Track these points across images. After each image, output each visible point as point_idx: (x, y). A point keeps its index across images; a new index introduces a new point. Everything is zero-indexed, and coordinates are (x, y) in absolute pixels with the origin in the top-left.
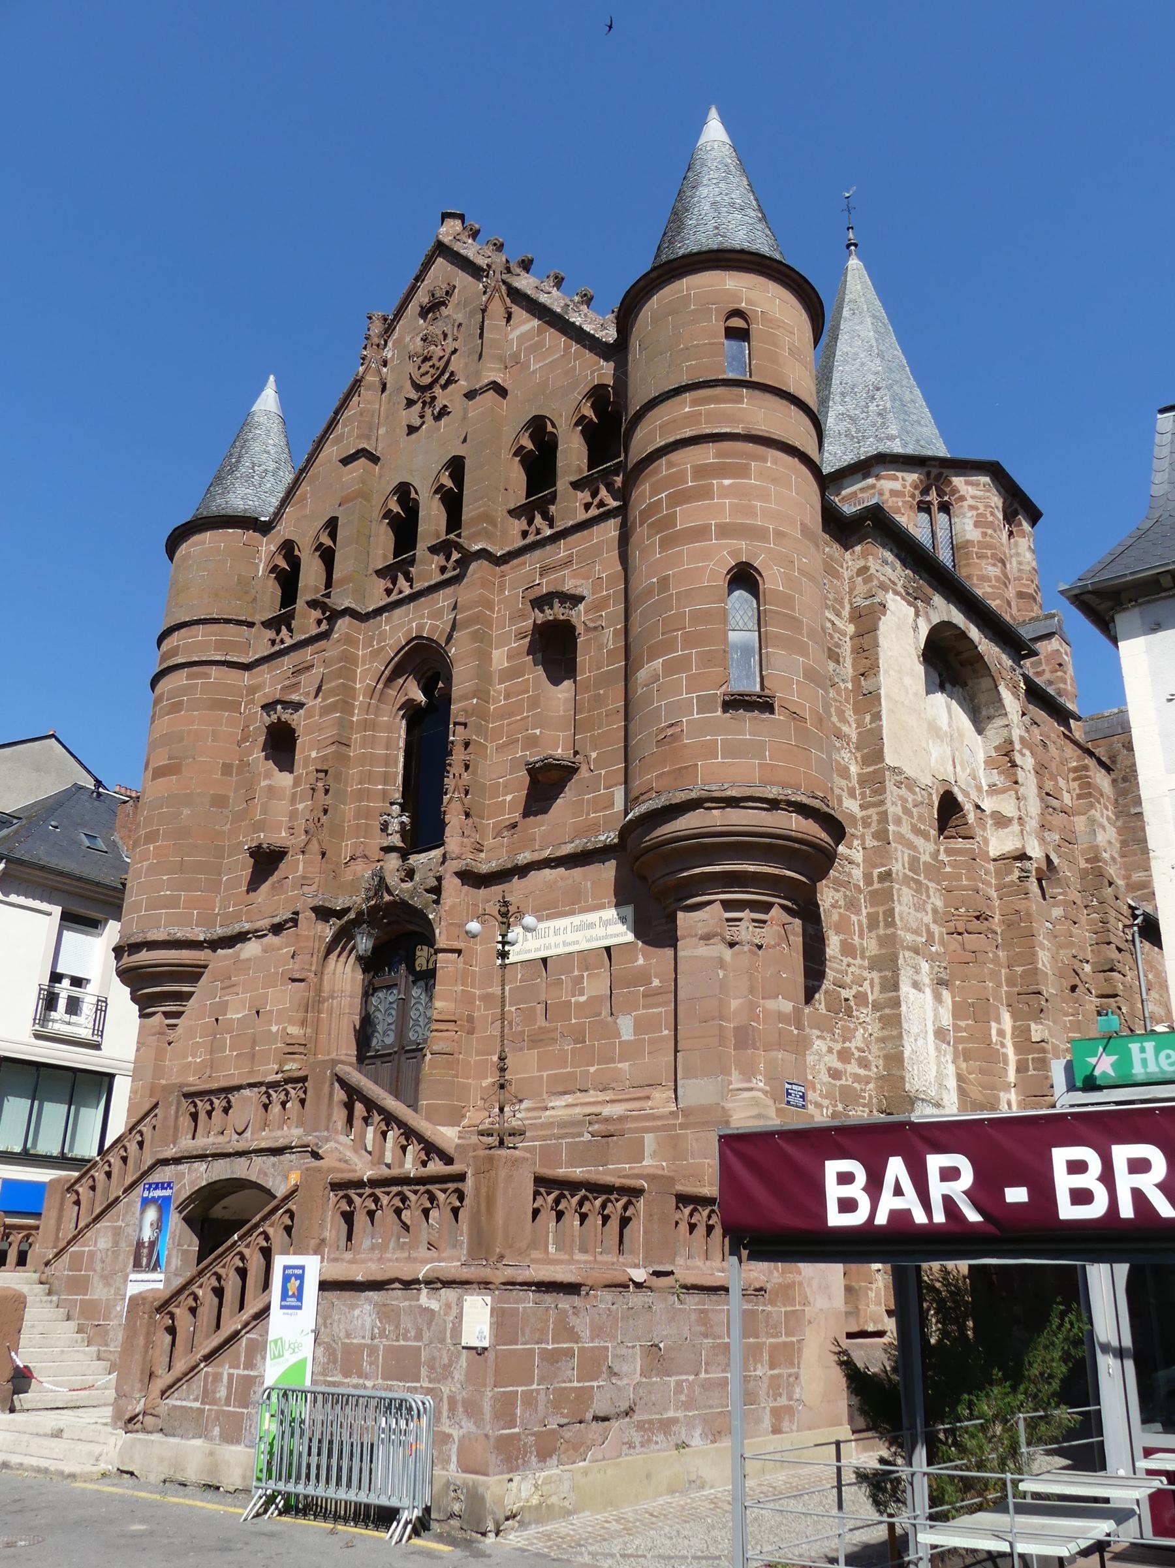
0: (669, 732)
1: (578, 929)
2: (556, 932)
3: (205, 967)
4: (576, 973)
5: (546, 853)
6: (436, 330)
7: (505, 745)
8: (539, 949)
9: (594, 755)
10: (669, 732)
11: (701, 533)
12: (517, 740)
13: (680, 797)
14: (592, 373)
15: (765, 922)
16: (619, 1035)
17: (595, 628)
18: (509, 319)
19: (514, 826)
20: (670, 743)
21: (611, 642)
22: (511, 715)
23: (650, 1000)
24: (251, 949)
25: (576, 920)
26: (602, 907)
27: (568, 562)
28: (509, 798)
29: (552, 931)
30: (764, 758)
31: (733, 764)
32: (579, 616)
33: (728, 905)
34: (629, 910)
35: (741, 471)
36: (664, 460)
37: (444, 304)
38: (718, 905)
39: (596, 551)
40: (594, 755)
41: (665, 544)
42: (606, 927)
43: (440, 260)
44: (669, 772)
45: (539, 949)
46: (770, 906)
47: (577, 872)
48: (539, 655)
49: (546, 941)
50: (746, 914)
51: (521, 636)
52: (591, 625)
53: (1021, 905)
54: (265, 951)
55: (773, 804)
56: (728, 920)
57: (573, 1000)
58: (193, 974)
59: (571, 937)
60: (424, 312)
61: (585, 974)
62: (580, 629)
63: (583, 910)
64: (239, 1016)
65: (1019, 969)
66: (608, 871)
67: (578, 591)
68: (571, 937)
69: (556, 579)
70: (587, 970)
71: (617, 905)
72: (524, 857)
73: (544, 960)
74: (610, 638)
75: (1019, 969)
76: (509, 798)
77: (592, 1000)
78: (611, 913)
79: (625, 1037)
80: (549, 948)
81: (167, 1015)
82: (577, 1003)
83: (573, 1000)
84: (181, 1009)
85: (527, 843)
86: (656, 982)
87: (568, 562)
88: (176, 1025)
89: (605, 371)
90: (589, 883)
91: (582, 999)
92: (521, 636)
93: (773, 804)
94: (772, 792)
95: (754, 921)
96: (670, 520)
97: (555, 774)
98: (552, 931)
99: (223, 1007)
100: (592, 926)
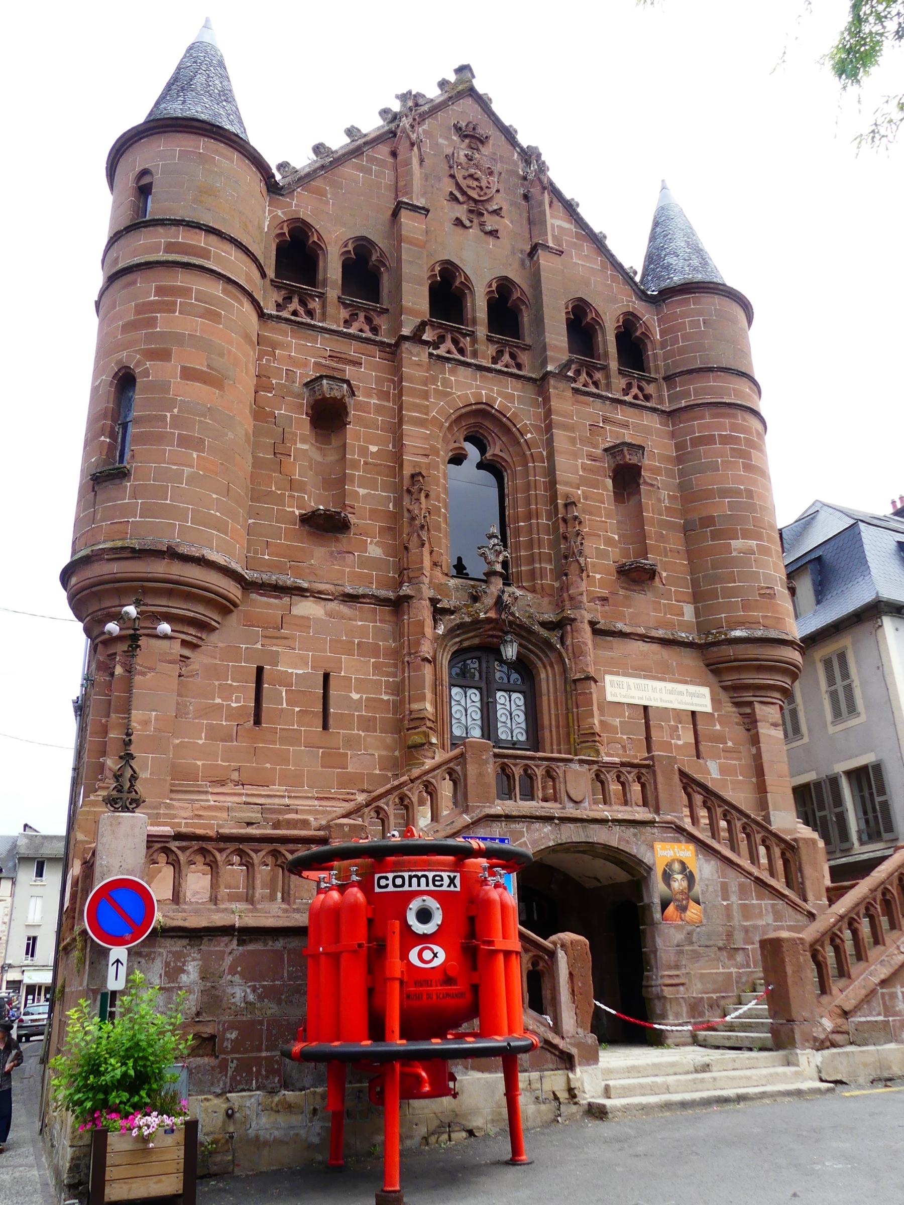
1: (671, 692)
2: (654, 690)
3: (235, 605)
5: (642, 631)
8: (642, 699)
12: (600, 536)
16: (709, 773)
21: (667, 501)
22: (591, 514)
23: (728, 755)
24: (306, 608)
25: (670, 686)
38: (778, 706)
40: (664, 574)
45: (642, 699)
54: (330, 614)
57: (673, 741)
58: (226, 607)
61: (680, 726)
64: (301, 672)
73: (646, 708)
77: (685, 744)
79: (714, 776)
81: (184, 643)
82: (676, 745)
83: (673, 741)
84: (200, 643)
86: (730, 744)
88: (188, 658)
91: (680, 743)
99: (274, 659)
100: (681, 693)
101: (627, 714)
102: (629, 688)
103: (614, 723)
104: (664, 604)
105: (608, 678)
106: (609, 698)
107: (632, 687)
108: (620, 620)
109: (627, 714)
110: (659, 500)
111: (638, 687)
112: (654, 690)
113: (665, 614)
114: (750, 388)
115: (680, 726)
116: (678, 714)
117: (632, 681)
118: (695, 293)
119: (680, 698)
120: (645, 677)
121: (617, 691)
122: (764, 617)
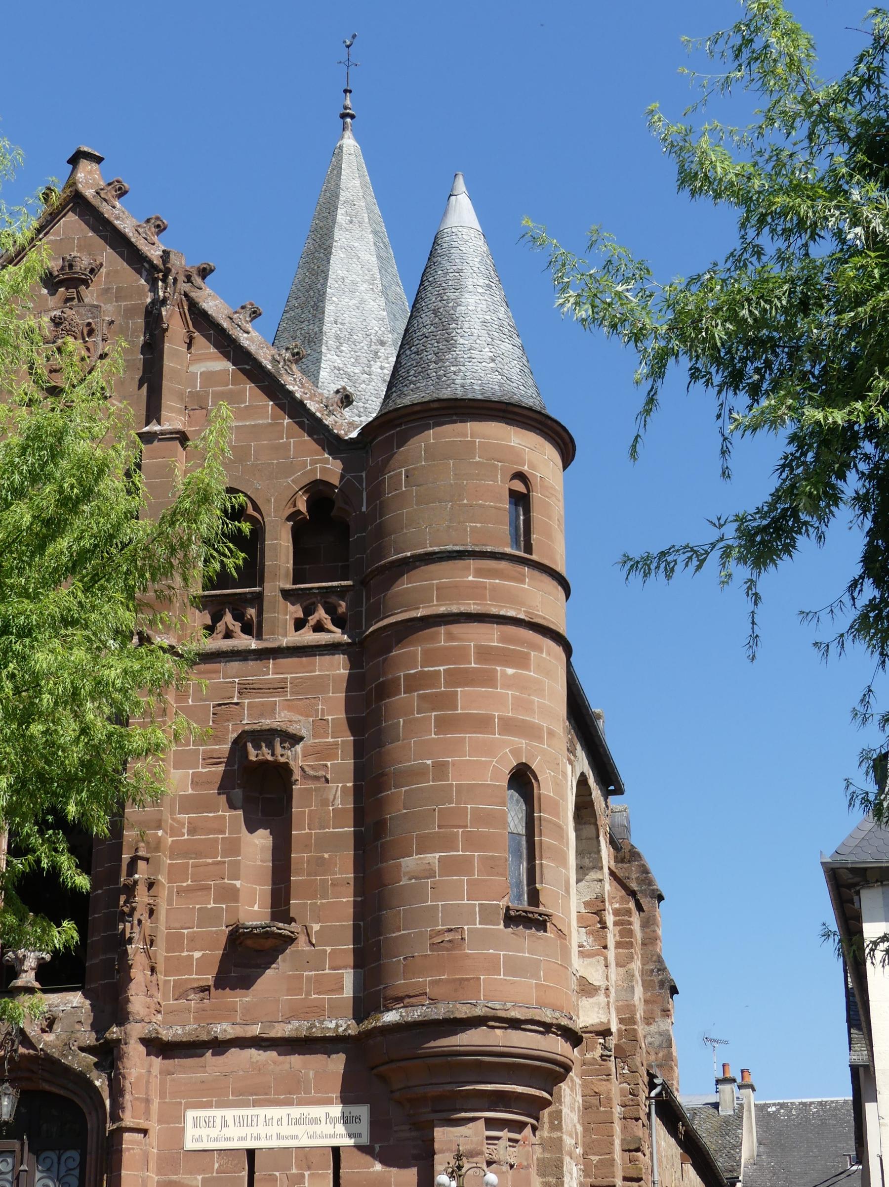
0: (448, 937)
1: (298, 1122)
2: (268, 1122)
4: (294, 1171)
5: (255, 1030)
6: (76, 317)
7: (188, 890)
8: (245, 1139)
9: (316, 927)
10: (448, 937)
11: (482, 723)
12: (208, 888)
13: (463, 1012)
14: (314, 462)
15: (517, 1141)
17: (316, 778)
18: (189, 346)
19: (205, 989)
20: (448, 950)
21: (338, 801)
25: (296, 1112)
26: (328, 1102)
27: (279, 688)
28: (197, 955)
29: (261, 1120)
30: (539, 978)
31: (514, 982)
32: (296, 757)
33: (491, 1124)
34: (363, 1111)
35: (521, 661)
36: (442, 629)
37: (86, 282)
39: (318, 686)
40: (316, 927)
41: (443, 724)
42: (320, 1123)
43: (71, 218)
44: (447, 981)
45: (245, 1139)
46: (523, 1125)
47: (296, 1060)
48: (238, 793)
49: (254, 1130)
50: (505, 1134)
51: (211, 760)
52: (312, 773)
53: (601, 1087)
55: (547, 1028)
56: (488, 1138)
59: (287, 1130)
60: (51, 282)
61: (307, 1174)
62: (297, 775)
63: (302, 1103)
65: (595, 1158)
66: (337, 1063)
67: (292, 729)
68: (287, 1130)
69: (262, 704)
70: (309, 1168)
71: (346, 1099)
72: (224, 1030)
73: (251, 1154)
74: (339, 794)
75: (595, 1158)
76: (197, 955)
78: (336, 1110)
80: (258, 1138)
85: (227, 1013)
87: (279, 688)
89: (331, 469)
90: (311, 1073)
92: (211, 760)
93: (547, 1028)
94: (547, 1016)
95: (510, 1140)
96: (450, 701)
97: (269, 943)
98: (261, 1120)
100: (315, 1121)
101: (216, 1166)
102: (225, 1124)
103: (194, 1183)
104: (309, 978)
105: (191, 1114)
106: (189, 1145)
107: (230, 1122)
108: (220, 1019)
109: (216, 1166)
110: (325, 803)
111: (240, 1122)
112: (268, 1122)
113: (308, 993)
114: (479, 573)
115: (307, 1174)
116: (305, 1155)
117: (230, 1114)
118: (400, 425)
119: (312, 1128)
120: (256, 1104)
121: (203, 1132)
122: (433, 983)
